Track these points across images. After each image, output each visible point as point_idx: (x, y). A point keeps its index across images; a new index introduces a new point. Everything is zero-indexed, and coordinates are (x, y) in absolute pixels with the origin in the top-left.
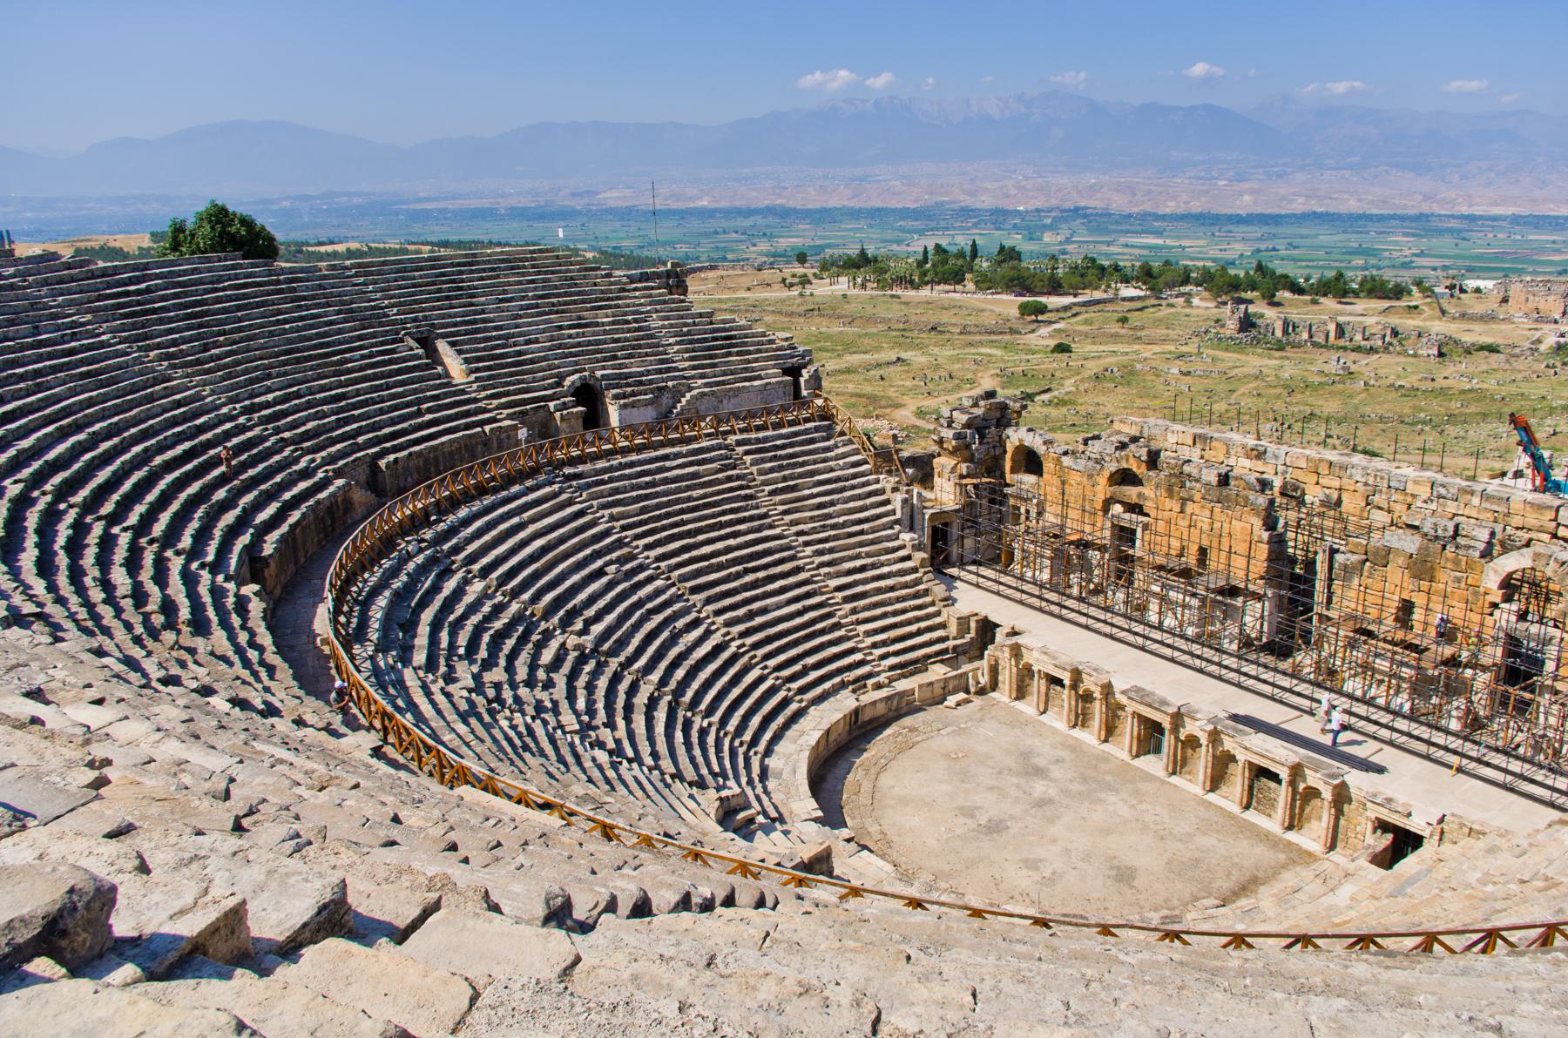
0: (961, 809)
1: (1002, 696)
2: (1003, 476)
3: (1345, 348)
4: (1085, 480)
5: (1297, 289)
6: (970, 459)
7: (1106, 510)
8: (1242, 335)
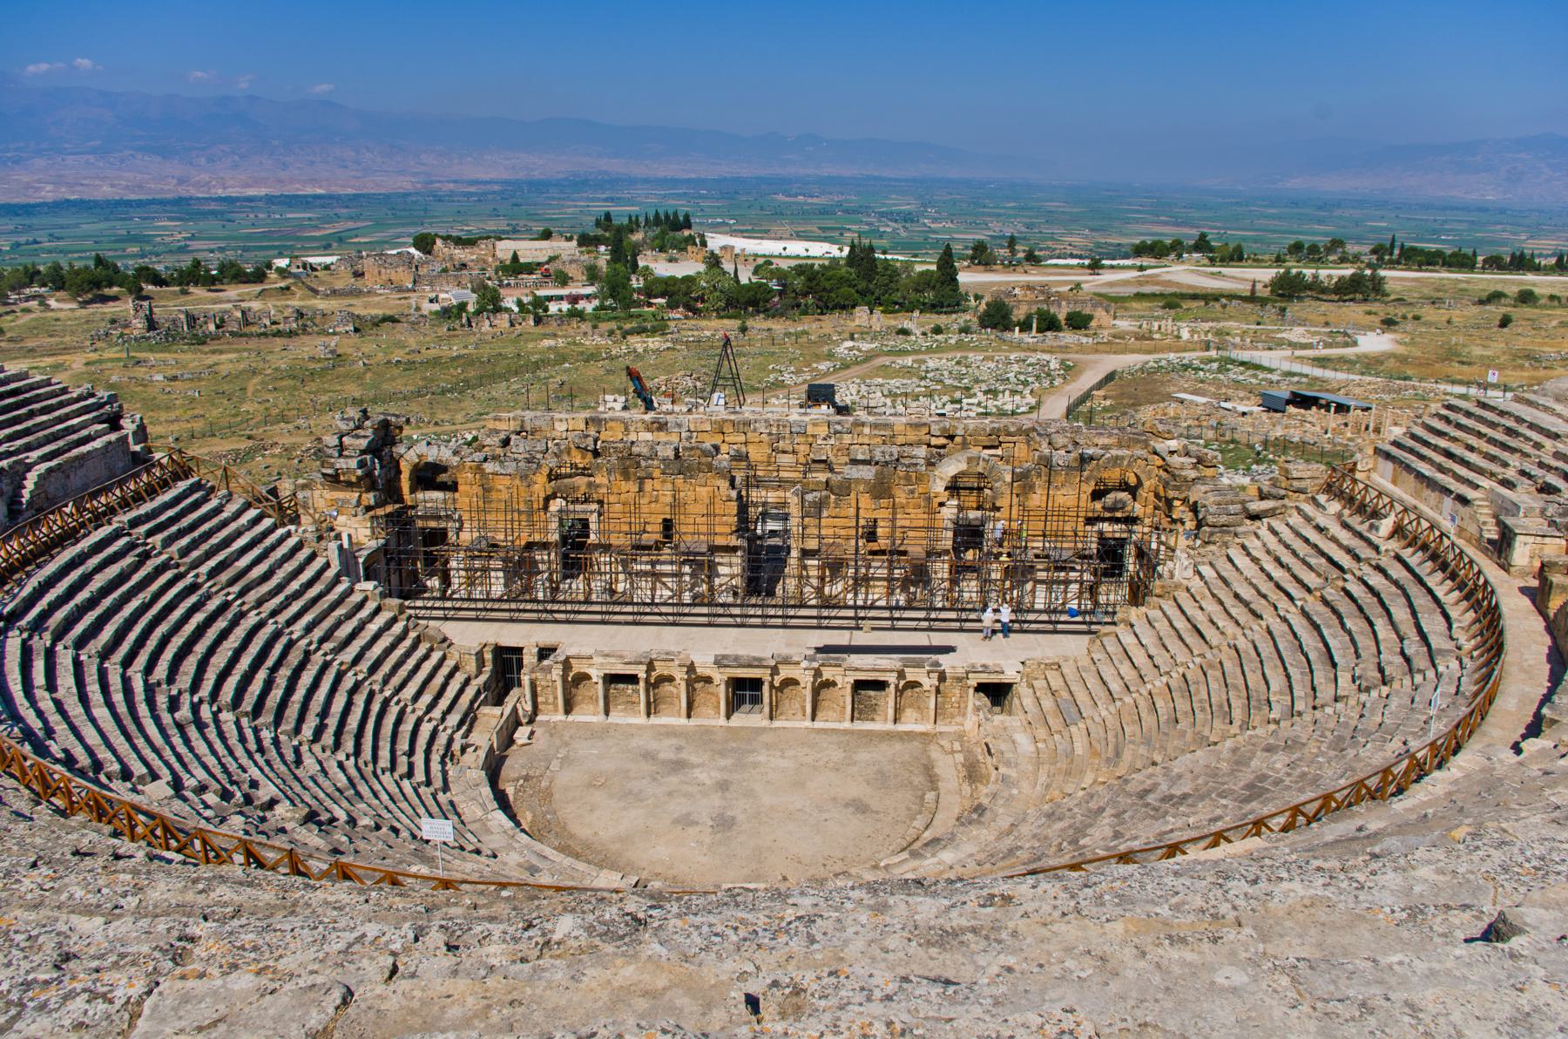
0: (676, 821)
1: (552, 715)
2: (401, 500)
3: (265, 334)
4: (517, 482)
5: (158, 281)
6: (372, 487)
7: (546, 508)
8: (151, 334)
